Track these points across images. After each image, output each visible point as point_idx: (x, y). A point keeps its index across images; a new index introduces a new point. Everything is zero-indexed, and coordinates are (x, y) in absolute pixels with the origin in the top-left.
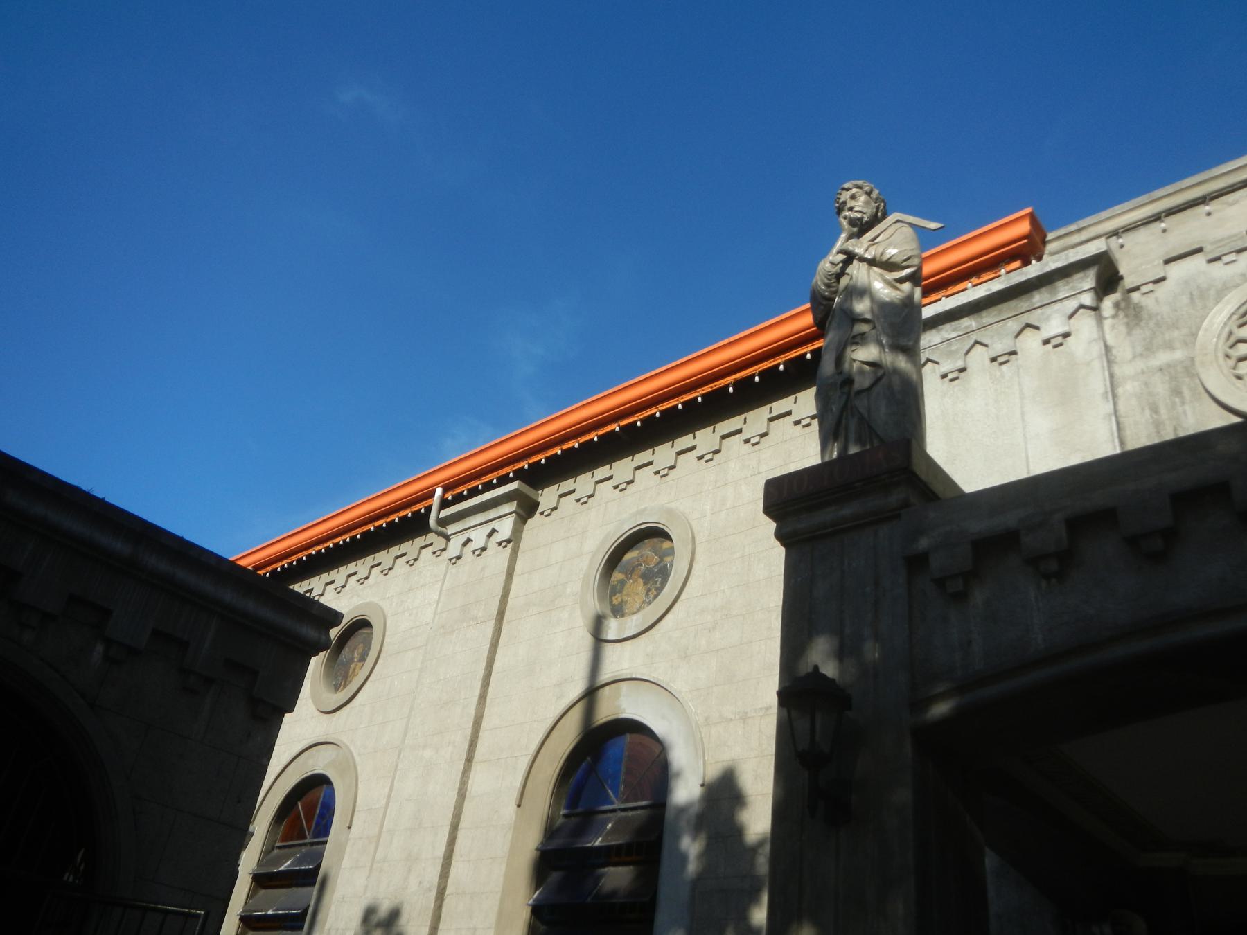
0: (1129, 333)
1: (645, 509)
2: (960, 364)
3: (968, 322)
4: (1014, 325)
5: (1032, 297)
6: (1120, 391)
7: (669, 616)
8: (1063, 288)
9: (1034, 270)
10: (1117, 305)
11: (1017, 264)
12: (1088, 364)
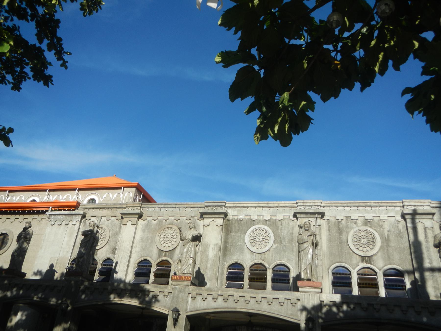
0: (83, 227)
1: (6, 229)
2: (61, 223)
3: (64, 216)
4: (70, 219)
5: (73, 216)
6: (78, 236)
7: (4, 253)
8: (77, 216)
9: (73, 212)
10: (84, 221)
11: (74, 208)
12: (75, 231)
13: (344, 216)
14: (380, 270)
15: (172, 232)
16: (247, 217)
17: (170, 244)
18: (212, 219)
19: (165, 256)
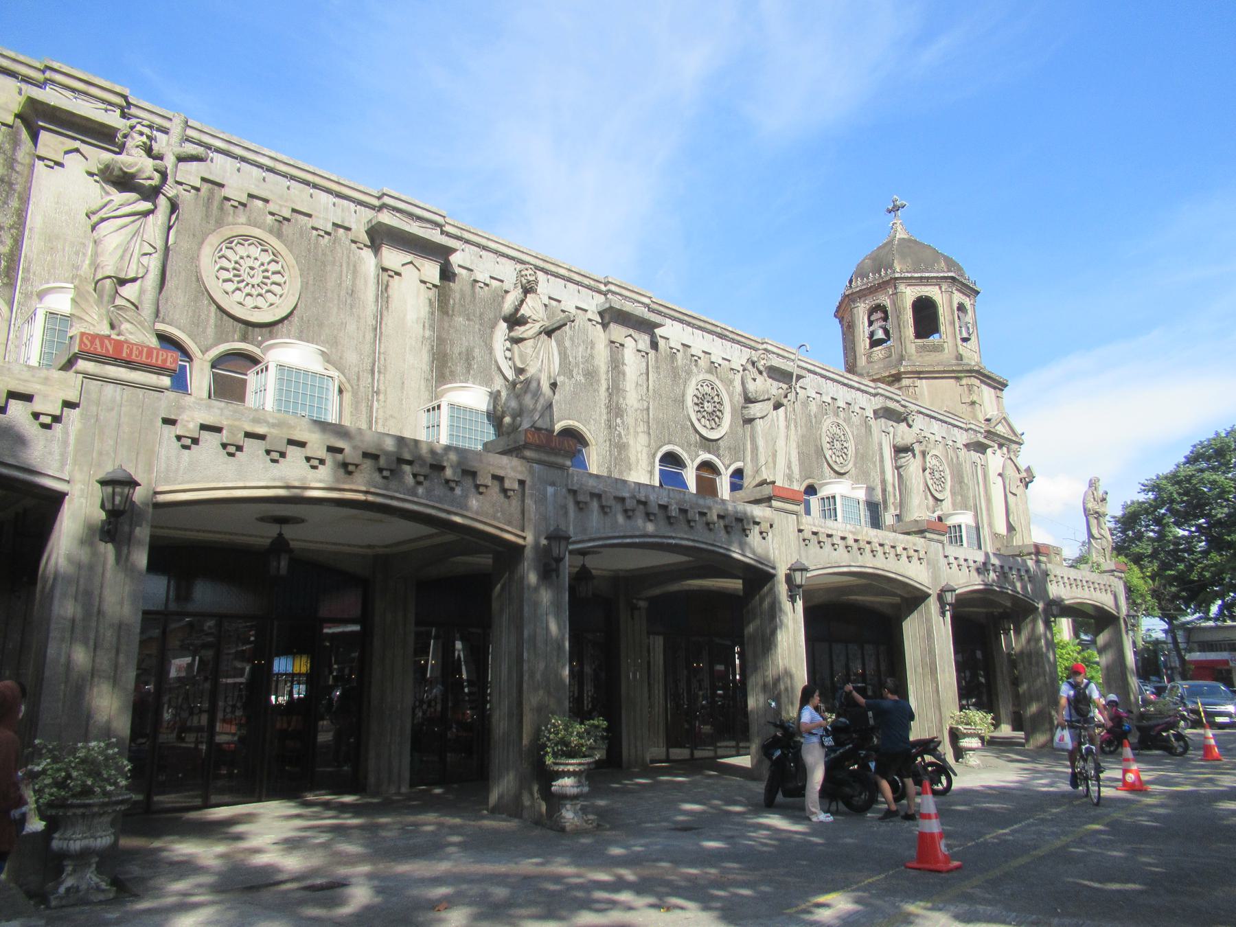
13: (682, 344)
14: (727, 469)
15: (266, 258)
16: (495, 283)
17: (260, 302)
18: (409, 258)
19: (244, 339)
